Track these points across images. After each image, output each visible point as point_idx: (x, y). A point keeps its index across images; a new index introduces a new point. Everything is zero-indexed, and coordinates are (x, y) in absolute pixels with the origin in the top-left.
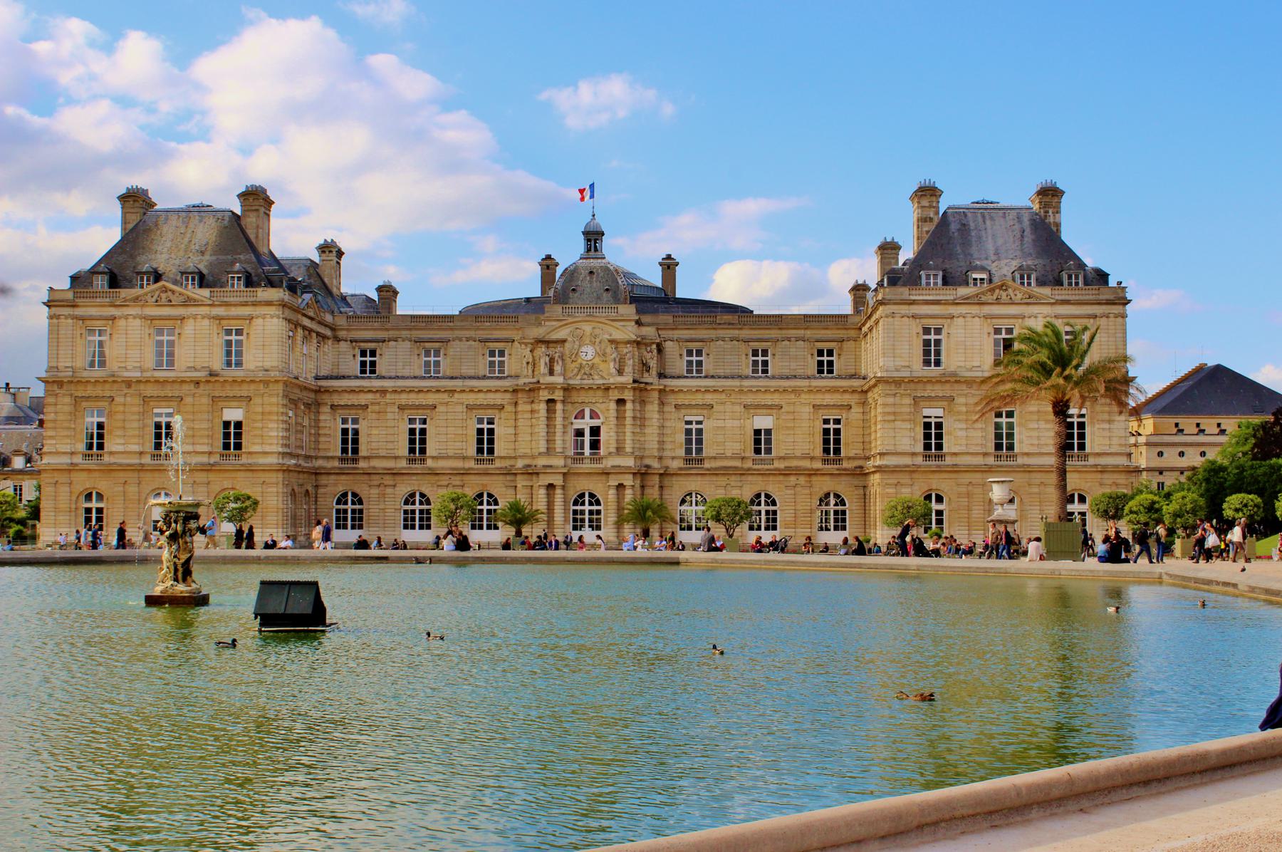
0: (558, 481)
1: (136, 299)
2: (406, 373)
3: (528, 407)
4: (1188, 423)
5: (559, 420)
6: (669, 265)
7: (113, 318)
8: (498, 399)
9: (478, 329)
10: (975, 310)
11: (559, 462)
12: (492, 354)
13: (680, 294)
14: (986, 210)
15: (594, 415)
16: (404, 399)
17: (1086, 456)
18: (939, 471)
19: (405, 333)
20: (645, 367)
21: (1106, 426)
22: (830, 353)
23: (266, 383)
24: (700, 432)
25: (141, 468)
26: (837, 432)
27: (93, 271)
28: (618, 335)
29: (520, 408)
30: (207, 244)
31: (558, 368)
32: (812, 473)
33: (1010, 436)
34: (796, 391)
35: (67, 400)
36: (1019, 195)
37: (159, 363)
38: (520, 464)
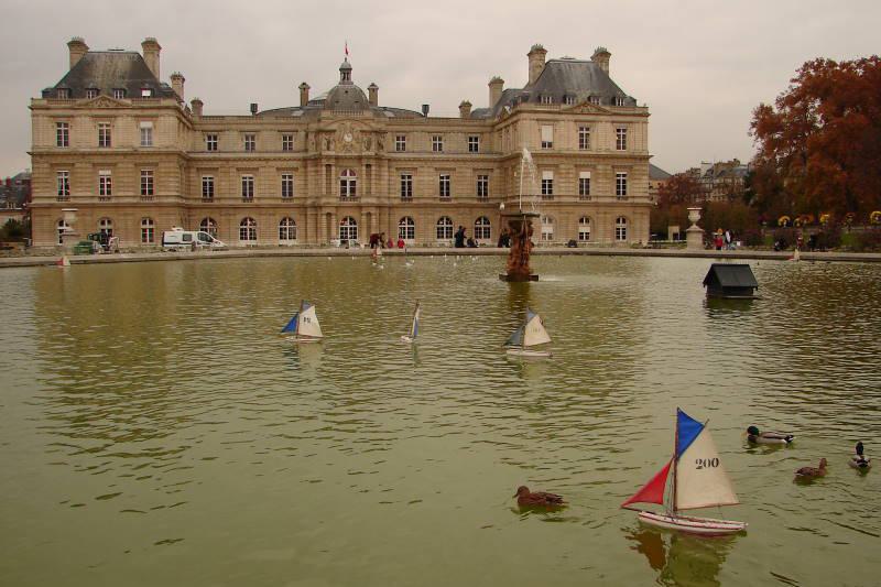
0: (333, 211)
1: (87, 104)
2: (235, 149)
3: (313, 169)
5: (333, 177)
6: (373, 89)
7: (72, 116)
9: (277, 124)
10: (570, 117)
11: (334, 201)
12: (285, 138)
13: (381, 104)
14: (569, 62)
15: (352, 174)
16: (240, 165)
17: (627, 198)
19: (234, 127)
20: (380, 146)
21: (636, 181)
22: (476, 139)
23: (168, 154)
24: (410, 183)
25: (93, 206)
26: (486, 184)
27: (57, 88)
28: (365, 128)
29: (309, 169)
30: (126, 73)
31: (332, 146)
32: (472, 207)
33: (588, 187)
34: (464, 161)
35: (46, 165)
36: (586, 55)
37: (101, 143)
38: (309, 202)
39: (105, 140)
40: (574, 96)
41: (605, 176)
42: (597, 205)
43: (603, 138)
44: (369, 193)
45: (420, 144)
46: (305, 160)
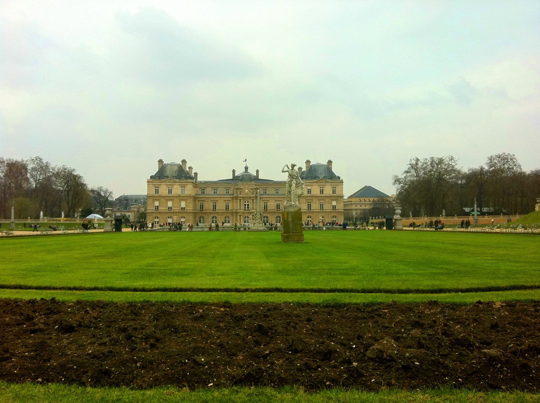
4: (362, 199)
6: (257, 172)
8: (230, 199)
14: (319, 166)
16: (212, 199)
18: (310, 212)
23: (190, 197)
39: (170, 191)
40: (318, 177)
41: (328, 203)
42: (325, 212)
43: (328, 190)
44: (253, 209)
45: (271, 191)
46: (233, 198)
